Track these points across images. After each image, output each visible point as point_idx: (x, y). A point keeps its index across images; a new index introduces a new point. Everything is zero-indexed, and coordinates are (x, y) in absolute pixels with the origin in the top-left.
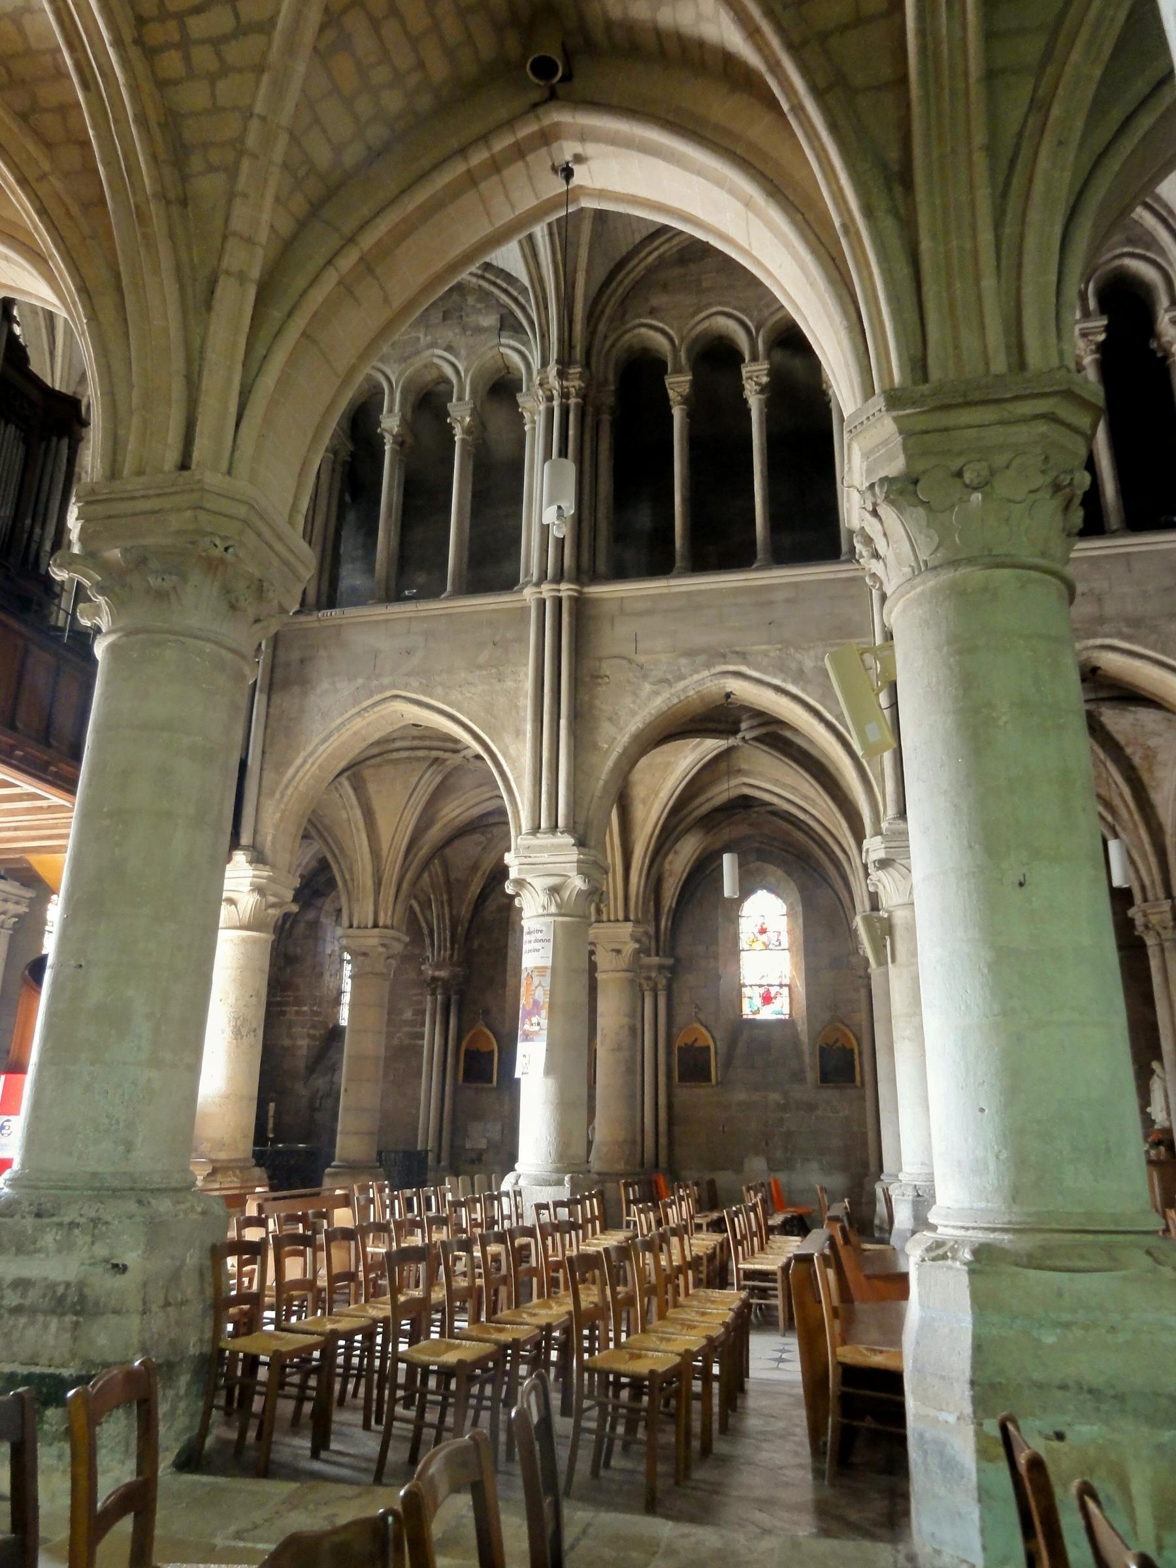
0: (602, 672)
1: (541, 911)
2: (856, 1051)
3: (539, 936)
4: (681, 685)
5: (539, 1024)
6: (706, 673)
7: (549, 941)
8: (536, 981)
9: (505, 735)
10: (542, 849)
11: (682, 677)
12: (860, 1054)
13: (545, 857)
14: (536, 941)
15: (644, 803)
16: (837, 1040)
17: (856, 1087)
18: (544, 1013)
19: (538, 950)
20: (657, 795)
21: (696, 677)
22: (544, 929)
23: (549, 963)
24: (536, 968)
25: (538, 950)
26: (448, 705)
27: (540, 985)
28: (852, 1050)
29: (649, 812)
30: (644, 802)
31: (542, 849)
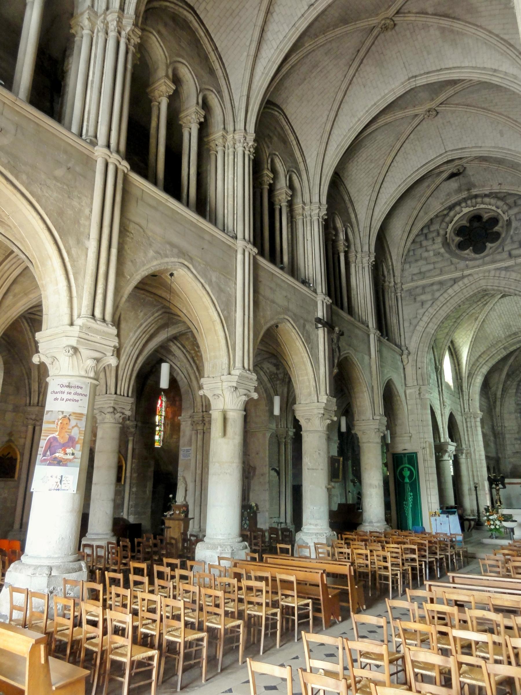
0: (130, 230)
1: (83, 373)
2: (18, 461)
3: (79, 391)
4: (166, 260)
5: (73, 454)
6: (176, 260)
7: (86, 396)
8: (73, 422)
9: (70, 238)
10: (97, 332)
11: (167, 256)
12: (21, 462)
13: (98, 338)
14: (76, 394)
15: (14, 296)
16: (9, 453)
17: (15, 481)
18: (79, 446)
19: (77, 401)
20: (26, 294)
21: (173, 260)
22: (84, 386)
23: (85, 412)
24: (74, 413)
25: (77, 401)
26: (30, 193)
27: (76, 426)
28: (16, 460)
29: (14, 304)
30: (14, 296)
31: (97, 332)
